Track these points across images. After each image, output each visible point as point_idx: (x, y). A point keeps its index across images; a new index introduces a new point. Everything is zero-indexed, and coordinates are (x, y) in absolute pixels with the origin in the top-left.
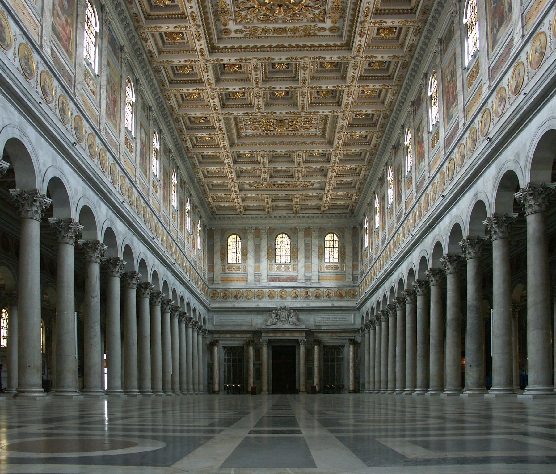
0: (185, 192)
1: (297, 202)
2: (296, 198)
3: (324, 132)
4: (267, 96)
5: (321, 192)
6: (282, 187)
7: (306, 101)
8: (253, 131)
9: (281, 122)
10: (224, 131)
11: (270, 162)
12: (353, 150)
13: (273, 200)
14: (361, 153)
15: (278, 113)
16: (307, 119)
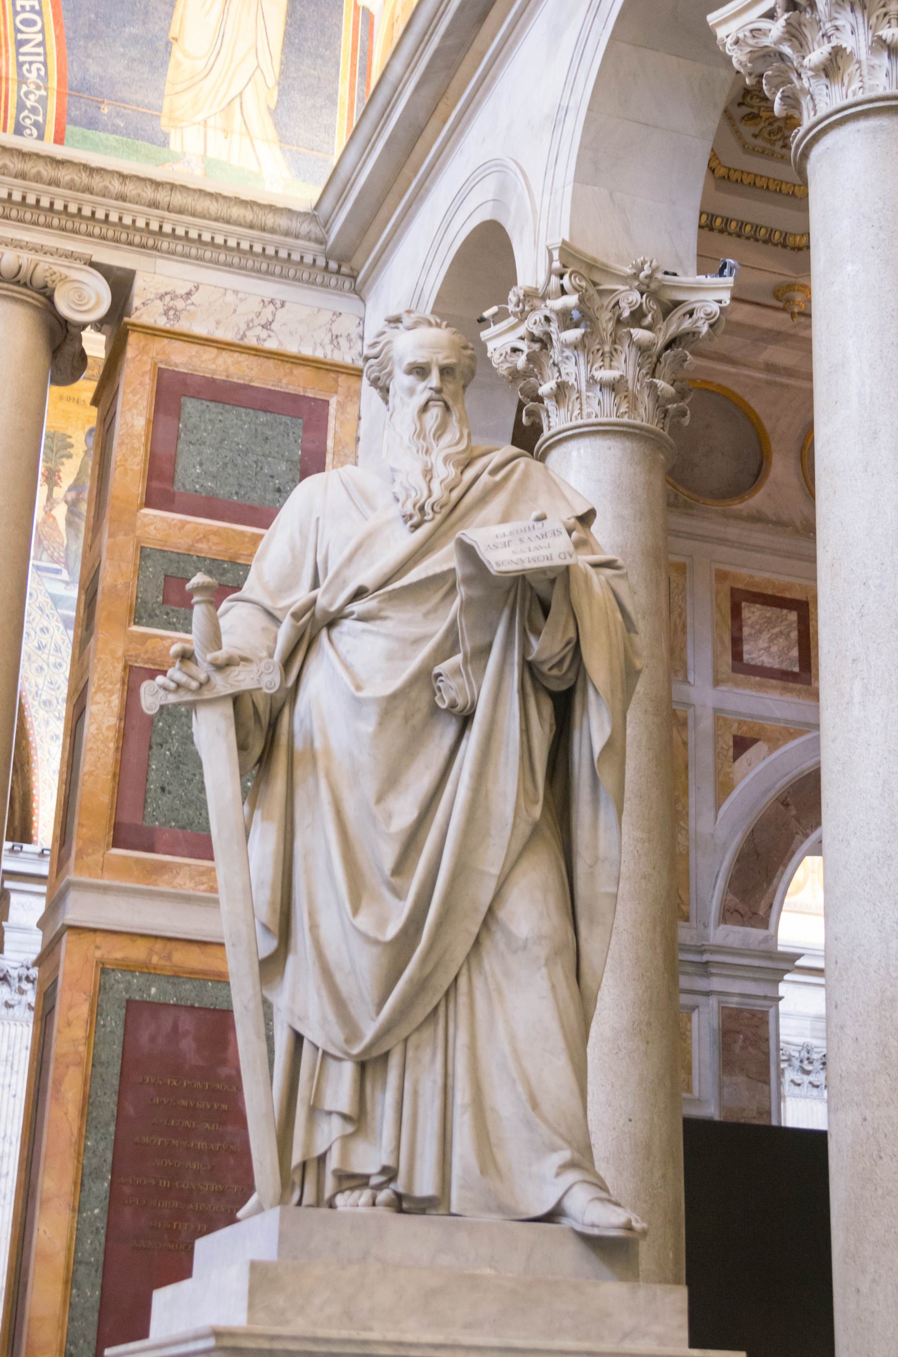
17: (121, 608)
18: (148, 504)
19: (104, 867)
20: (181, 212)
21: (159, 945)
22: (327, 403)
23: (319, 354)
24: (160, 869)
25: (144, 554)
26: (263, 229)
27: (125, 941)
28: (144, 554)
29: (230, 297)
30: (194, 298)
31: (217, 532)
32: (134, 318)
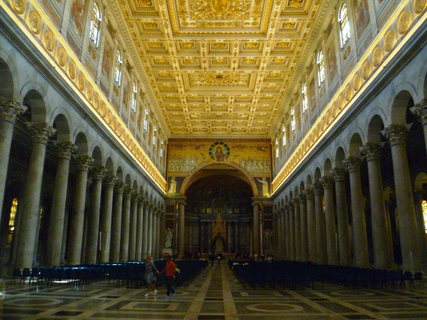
0: (154, 120)
1: (229, 127)
2: (229, 124)
3: (249, 84)
4: (210, 62)
5: (245, 121)
6: (218, 117)
7: (236, 65)
8: (200, 83)
9: (219, 77)
10: (182, 82)
11: (211, 101)
12: (267, 95)
13: (213, 125)
14: (273, 97)
15: (218, 72)
16: (237, 75)
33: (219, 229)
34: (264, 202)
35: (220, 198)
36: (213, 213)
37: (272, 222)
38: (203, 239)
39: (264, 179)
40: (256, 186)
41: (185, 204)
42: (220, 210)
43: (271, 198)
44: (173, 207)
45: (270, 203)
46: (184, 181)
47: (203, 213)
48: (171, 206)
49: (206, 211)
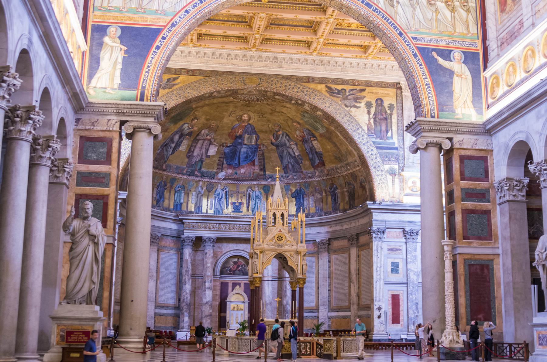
17: (460, 199)
18: (461, 180)
19: (463, 243)
20: (461, 127)
21: (472, 255)
22: (487, 157)
23: (485, 148)
24: (470, 243)
25: (462, 189)
26: (475, 127)
27: (467, 255)
28: (462, 189)
29: (469, 140)
30: (464, 141)
31: (472, 184)
32: (454, 147)
33: (280, 238)
34: (457, 138)
35: (242, 171)
36: (217, 211)
37: (487, 213)
38: (188, 287)
39: (457, 55)
40: (428, 80)
41: (157, 129)
42: (241, 204)
43: (485, 124)
44: (107, 142)
45: (481, 143)
46: (157, 43)
47: (191, 212)
48: (101, 140)
49: (198, 207)
